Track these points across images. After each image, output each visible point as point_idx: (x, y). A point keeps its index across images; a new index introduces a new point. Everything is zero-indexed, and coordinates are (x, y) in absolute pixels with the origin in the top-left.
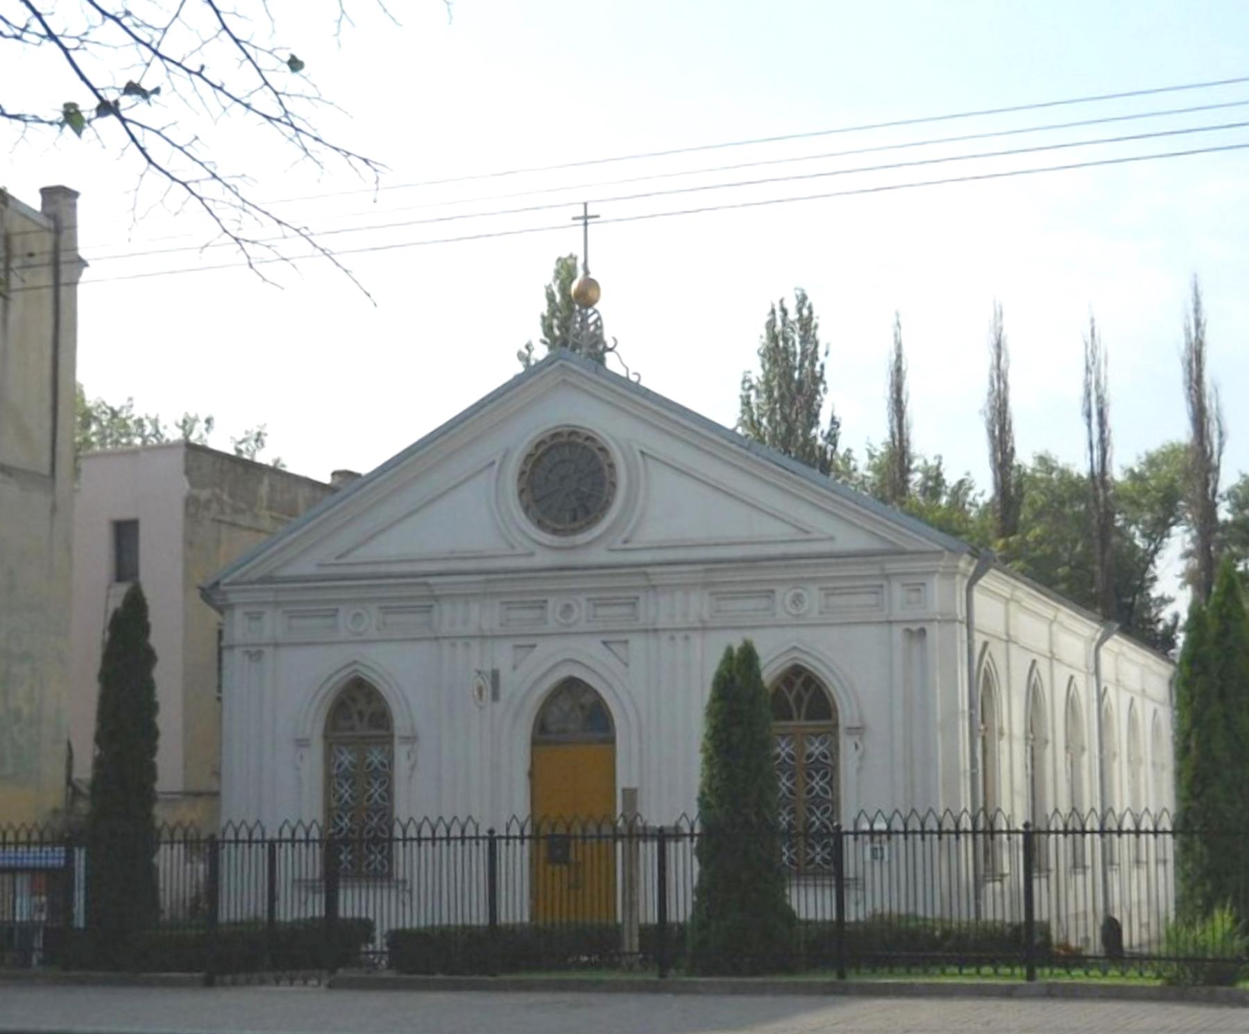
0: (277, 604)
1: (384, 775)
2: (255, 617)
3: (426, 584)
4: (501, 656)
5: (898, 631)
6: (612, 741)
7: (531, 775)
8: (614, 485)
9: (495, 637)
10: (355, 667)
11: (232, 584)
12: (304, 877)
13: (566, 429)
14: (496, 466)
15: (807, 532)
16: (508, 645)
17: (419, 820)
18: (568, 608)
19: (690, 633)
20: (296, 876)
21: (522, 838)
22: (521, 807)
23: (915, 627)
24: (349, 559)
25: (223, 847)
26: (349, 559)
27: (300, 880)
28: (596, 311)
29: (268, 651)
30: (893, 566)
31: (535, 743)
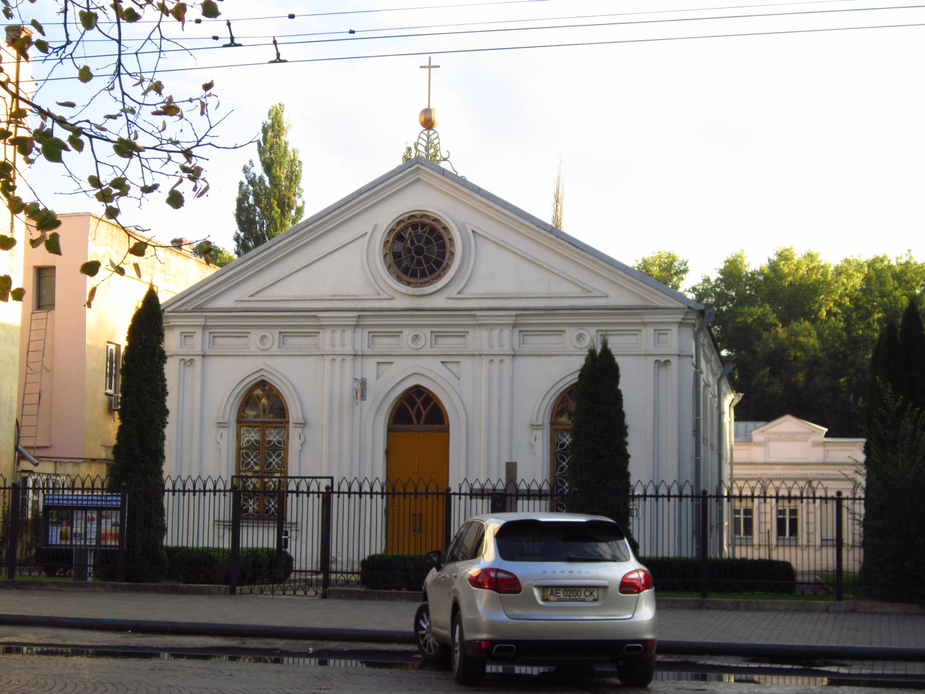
1: (280, 449)
2: (186, 336)
3: (315, 317)
4: (369, 369)
6: (447, 431)
7: (387, 453)
8: (452, 254)
9: (363, 355)
10: (260, 374)
11: (173, 311)
12: (222, 519)
13: (420, 213)
14: (368, 236)
15: (589, 291)
17: (215, 478)
18: (416, 338)
19: (504, 358)
20: (217, 518)
21: (680, 496)
22: (380, 472)
23: (663, 359)
24: (260, 296)
25: (287, 496)
27: (219, 521)
28: (435, 132)
29: (198, 360)
30: (648, 318)
31: (390, 430)
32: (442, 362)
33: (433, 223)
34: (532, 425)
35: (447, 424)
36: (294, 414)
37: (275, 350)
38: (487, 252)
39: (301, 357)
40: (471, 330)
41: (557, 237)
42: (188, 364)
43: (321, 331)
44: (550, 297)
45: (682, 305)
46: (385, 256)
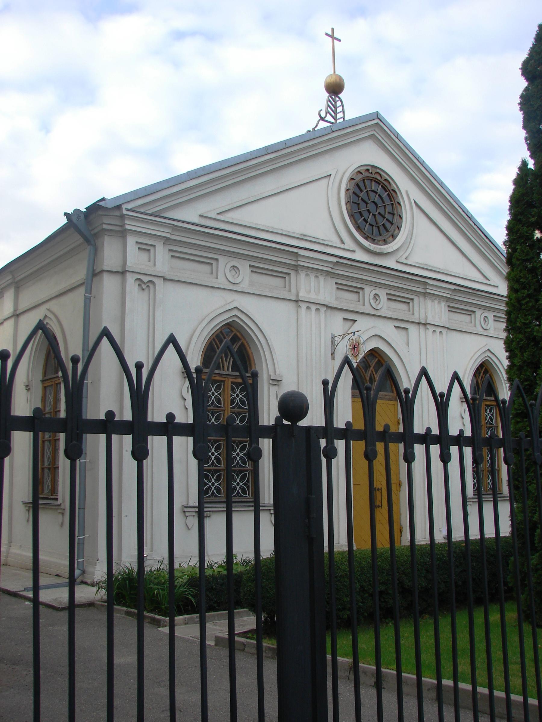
0: (167, 241)
16: (340, 316)
26: (227, 217)
32: (394, 326)
33: (385, 182)
34: (461, 398)
37: (245, 286)
39: (274, 299)
40: (416, 299)
41: (475, 224)
42: (144, 287)
43: (293, 273)
46: (346, 204)
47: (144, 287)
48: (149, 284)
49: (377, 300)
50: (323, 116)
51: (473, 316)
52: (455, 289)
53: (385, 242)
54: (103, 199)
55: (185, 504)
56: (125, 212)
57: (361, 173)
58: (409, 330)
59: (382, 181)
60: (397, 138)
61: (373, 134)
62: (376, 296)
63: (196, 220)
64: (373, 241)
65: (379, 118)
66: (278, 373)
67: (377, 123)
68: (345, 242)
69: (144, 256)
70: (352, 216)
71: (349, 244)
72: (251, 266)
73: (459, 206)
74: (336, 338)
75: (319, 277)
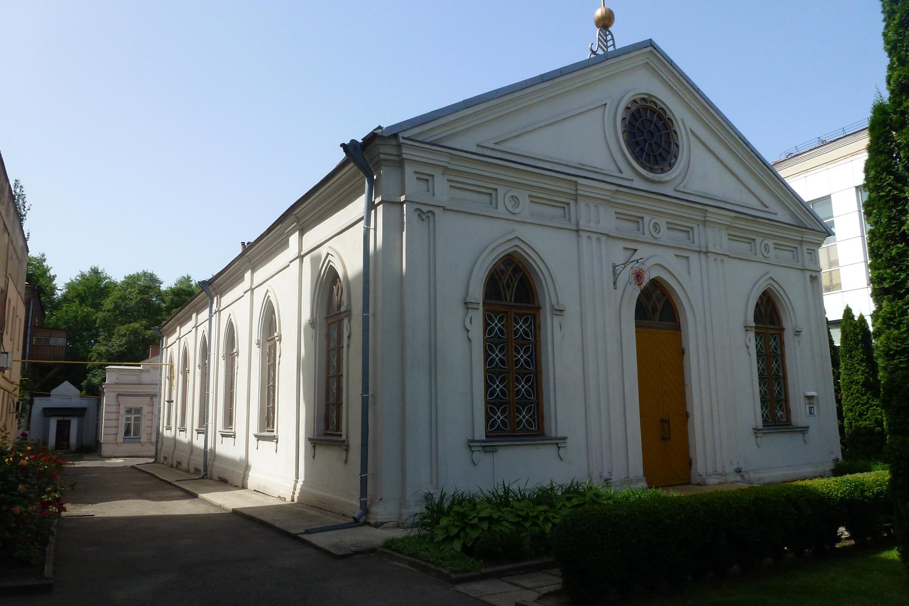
5: (808, 274)
11: (408, 139)
15: (766, 207)
26: (505, 147)
28: (610, 33)
32: (676, 255)
33: (660, 111)
34: (745, 327)
35: (678, 322)
36: (548, 299)
38: (698, 151)
42: (424, 217)
43: (572, 203)
44: (744, 206)
45: (824, 230)
47: (424, 217)
48: (429, 214)
49: (657, 229)
50: (595, 50)
51: (753, 244)
52: (735, 216)
53: (663, 171)
54: (380, 127)
55: (470, 438)
56: (401, 140)
57: (637, 103)
58: (690, 258)
59: (658, 109)
60: (671, 65)
61: (647, 63)
62: (656, 225)
63: (474, 150)
64: (651, 170)
65: (652, 46)
66: (560, 303)
67: (651, 51)
68: (622, 170)
69: (423, 185)
70: (629, 145)
71: (627, 173)
72: (530, 196)
73: (736, 133)
74: (617, 268)
75: (599, 206)
